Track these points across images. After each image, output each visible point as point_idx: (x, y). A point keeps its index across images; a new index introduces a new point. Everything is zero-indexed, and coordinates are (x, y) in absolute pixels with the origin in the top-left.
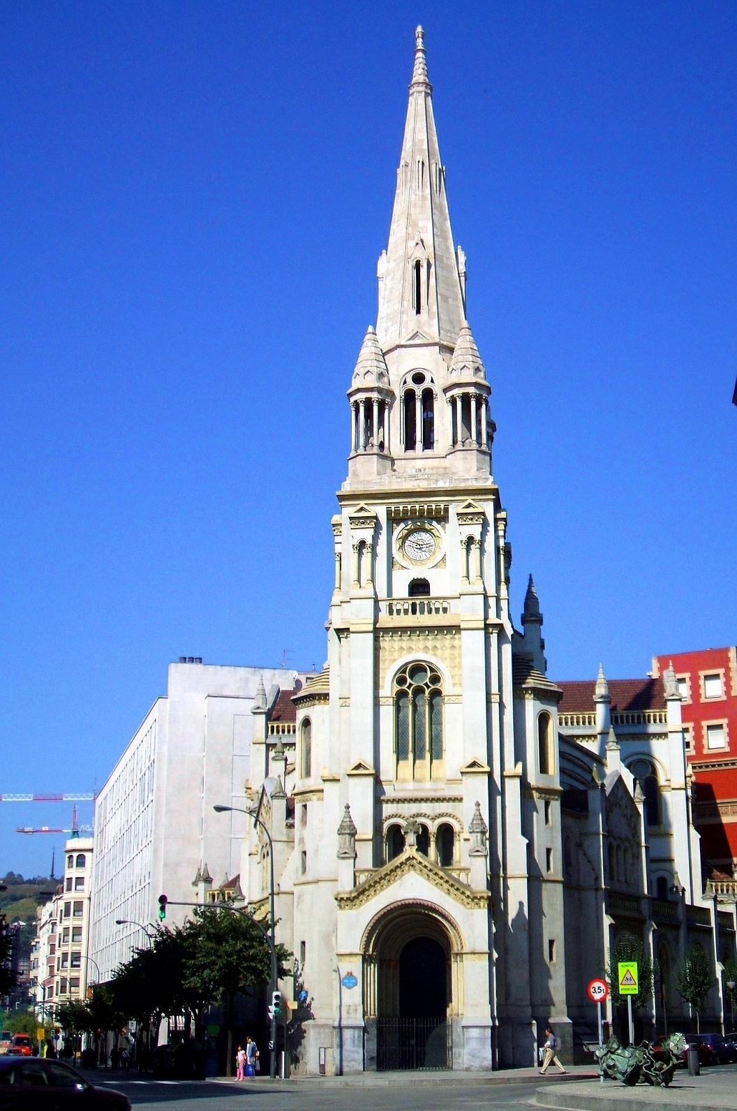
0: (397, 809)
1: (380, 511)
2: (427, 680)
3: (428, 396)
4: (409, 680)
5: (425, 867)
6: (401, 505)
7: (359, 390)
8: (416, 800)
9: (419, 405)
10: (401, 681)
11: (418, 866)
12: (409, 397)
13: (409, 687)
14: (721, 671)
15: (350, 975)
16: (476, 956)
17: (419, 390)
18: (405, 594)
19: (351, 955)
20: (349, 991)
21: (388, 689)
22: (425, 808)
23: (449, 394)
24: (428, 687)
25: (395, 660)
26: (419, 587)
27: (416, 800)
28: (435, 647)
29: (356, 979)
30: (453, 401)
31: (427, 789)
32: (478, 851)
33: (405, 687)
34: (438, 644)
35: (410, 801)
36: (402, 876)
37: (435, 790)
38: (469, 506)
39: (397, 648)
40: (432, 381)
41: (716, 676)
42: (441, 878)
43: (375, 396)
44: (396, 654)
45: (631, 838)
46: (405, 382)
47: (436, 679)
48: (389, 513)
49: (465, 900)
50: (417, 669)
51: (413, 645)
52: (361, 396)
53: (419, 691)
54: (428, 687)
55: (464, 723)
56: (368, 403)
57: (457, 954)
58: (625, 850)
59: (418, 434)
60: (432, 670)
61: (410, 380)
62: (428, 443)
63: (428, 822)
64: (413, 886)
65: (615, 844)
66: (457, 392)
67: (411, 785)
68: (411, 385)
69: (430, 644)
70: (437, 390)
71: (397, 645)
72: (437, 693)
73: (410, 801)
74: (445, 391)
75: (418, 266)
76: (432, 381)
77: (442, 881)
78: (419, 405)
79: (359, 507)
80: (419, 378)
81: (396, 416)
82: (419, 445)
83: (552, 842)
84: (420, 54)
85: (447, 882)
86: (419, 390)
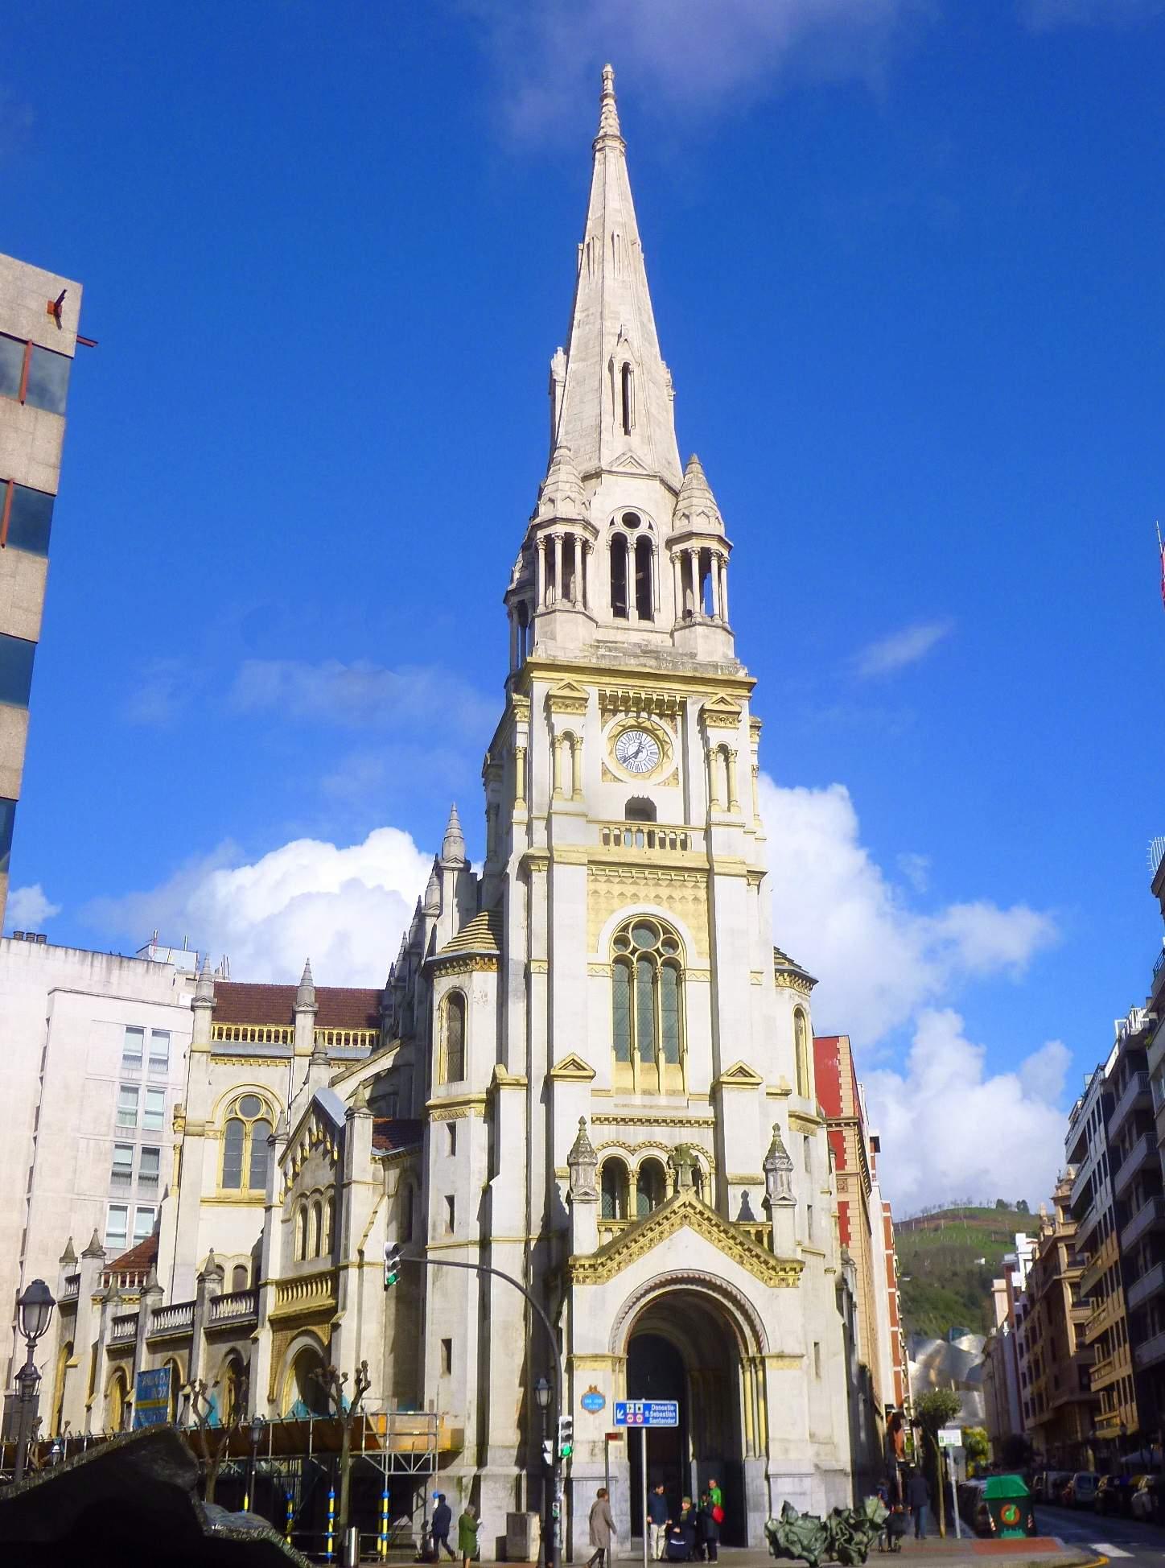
0: (618, 1132)
1: (593, 693)
2: (659, 944)
3: (645, 548)
4: (633, 944)
5: (709, 1219)
6: (616, 686)
7: (554, 521)
9: (631, 559)
10: (621, 941)
12: (618, 545)
13: (633, 953)
15: (593, 1390)
16: (787, 1361)
17: (632, 537)
18: (622, 817)
19: (596, 1357)
20: (591, 1417)
21: (607, 952)
22: (661, 1134)
23: (677, 548)
24: (657, 950)
25: (613, 911)
26: (641, 810)
28: (670, 897)
29: (603, 1397)
30: (686, 558)
31: (663, 1105)
32: (784, 1198)
33: (627, 953)
34: (677, 894)
36: (671, 1233)
37: (676, 1108)
38: (722, 700)
39: (616, 893)
40: (650, 527)
42: (734, 1238)
43: (578, 531)
44: (616, 902)
46: (612, 523)
47: (671, 944)
48: (602, 697)
49: (766, 1273)
50: (645, 925)
51: (642, 891)
52: (560, 529)
53: (646, 958)
54: (661, 955)
56: (569, 541)
57: (752, 1360)
59: (632, 593)
60: (666, 931)
61: (619, 520)
62: (645, 612)
64: (687, 1250)
66: (695, 545)
67: (638, 1099)
69: (664, 892)
70: (658, 540)
71: (617, 889)
72: (673, 964)
74: (670, 543)
75: (626, 370)
76: (650, 527)
78: (631, 559)
79: (562, 684)
80: (631, 520)
81: (599, 565)
82: (633, 612)
83: (812, 1197)
84: (610, 101)
86: (632, 537)
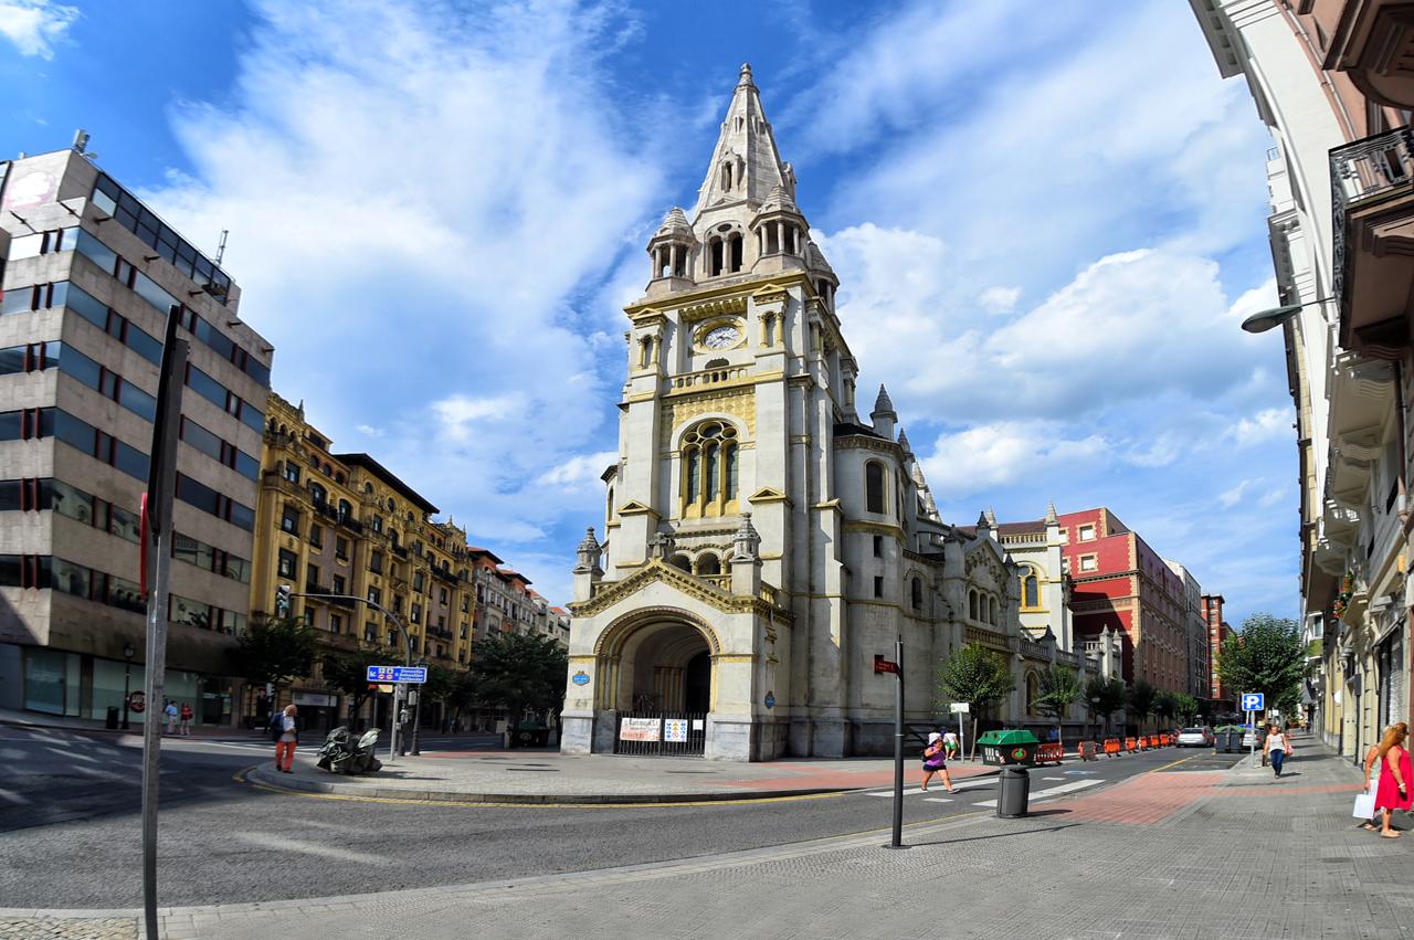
5: (673, 575)
8: (703, 534)
11: (665, 576)
12: (716, 246)
14: (1093, 524)
17: (724, 236)
27: (703, 534)
35: (696, 534)
41: (1090, 527)
42: (693, 585)
45: (999, 591)
55: (761, 462)
58: (992, 600)
63: (718, 553)
65: (979, 592)
68: (715, 232)
73: (696, 534)
77: (692, 588)
80: (725, 227)
85: (699, 588)
86: (724, 236)
